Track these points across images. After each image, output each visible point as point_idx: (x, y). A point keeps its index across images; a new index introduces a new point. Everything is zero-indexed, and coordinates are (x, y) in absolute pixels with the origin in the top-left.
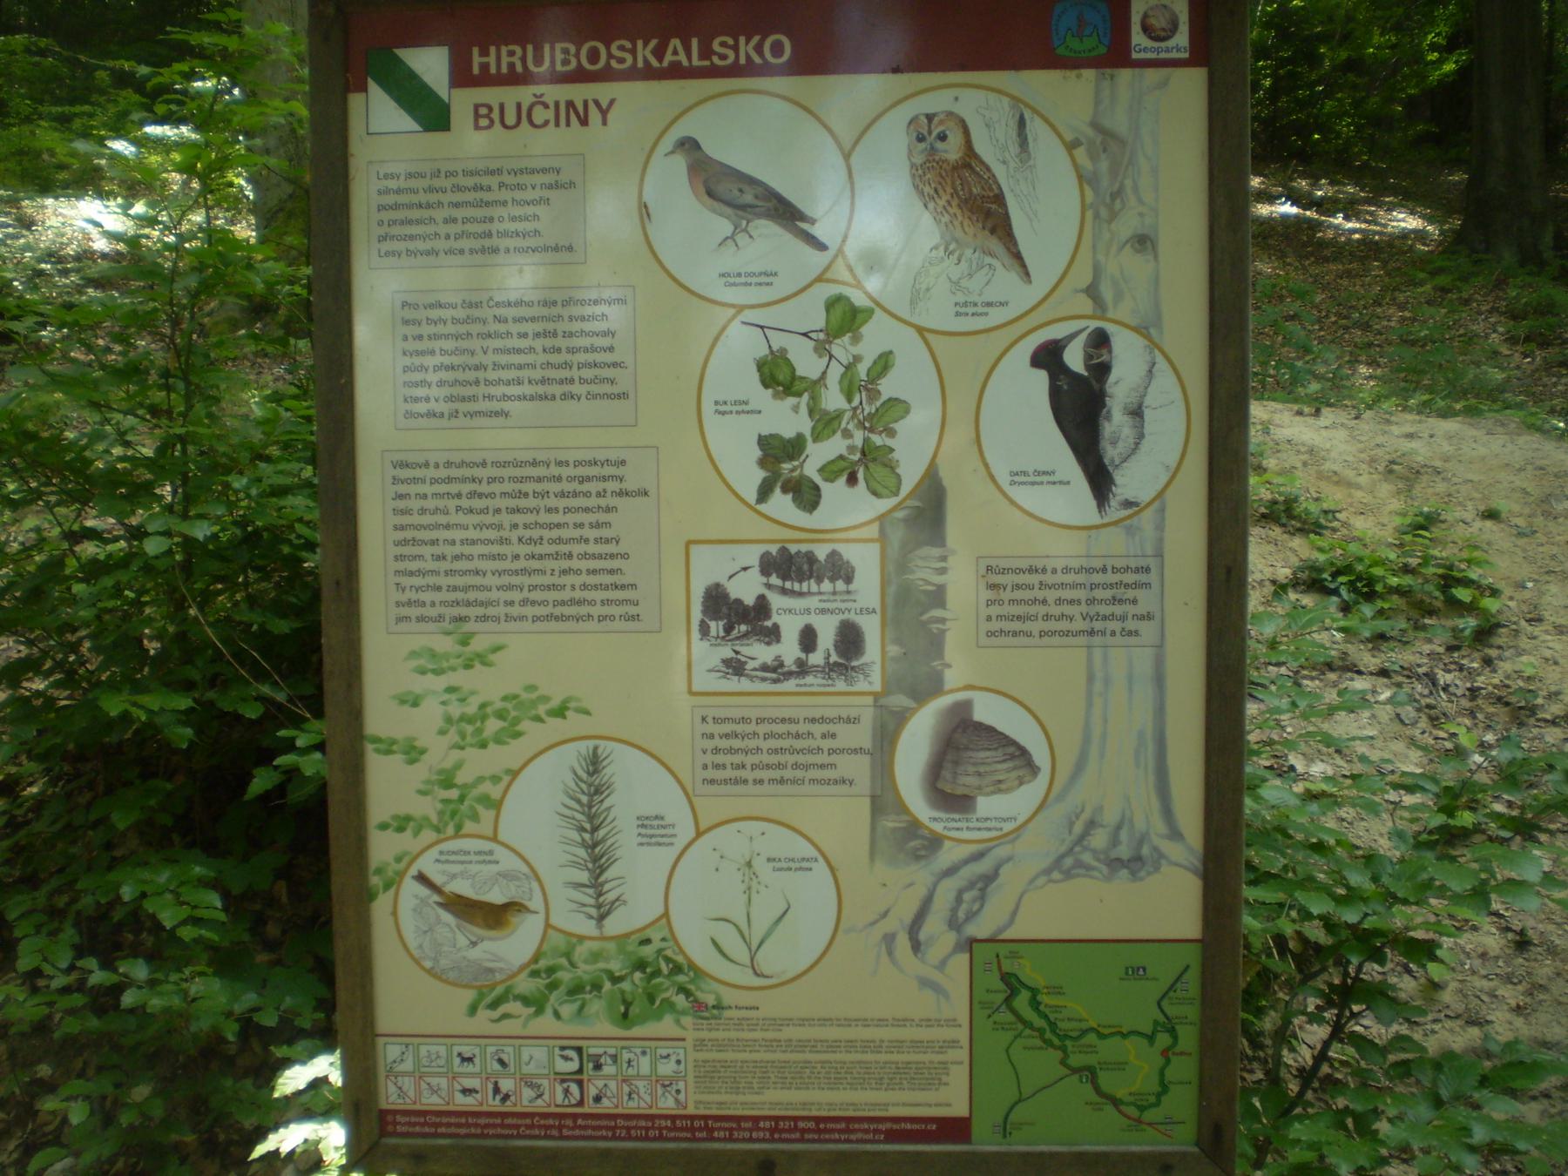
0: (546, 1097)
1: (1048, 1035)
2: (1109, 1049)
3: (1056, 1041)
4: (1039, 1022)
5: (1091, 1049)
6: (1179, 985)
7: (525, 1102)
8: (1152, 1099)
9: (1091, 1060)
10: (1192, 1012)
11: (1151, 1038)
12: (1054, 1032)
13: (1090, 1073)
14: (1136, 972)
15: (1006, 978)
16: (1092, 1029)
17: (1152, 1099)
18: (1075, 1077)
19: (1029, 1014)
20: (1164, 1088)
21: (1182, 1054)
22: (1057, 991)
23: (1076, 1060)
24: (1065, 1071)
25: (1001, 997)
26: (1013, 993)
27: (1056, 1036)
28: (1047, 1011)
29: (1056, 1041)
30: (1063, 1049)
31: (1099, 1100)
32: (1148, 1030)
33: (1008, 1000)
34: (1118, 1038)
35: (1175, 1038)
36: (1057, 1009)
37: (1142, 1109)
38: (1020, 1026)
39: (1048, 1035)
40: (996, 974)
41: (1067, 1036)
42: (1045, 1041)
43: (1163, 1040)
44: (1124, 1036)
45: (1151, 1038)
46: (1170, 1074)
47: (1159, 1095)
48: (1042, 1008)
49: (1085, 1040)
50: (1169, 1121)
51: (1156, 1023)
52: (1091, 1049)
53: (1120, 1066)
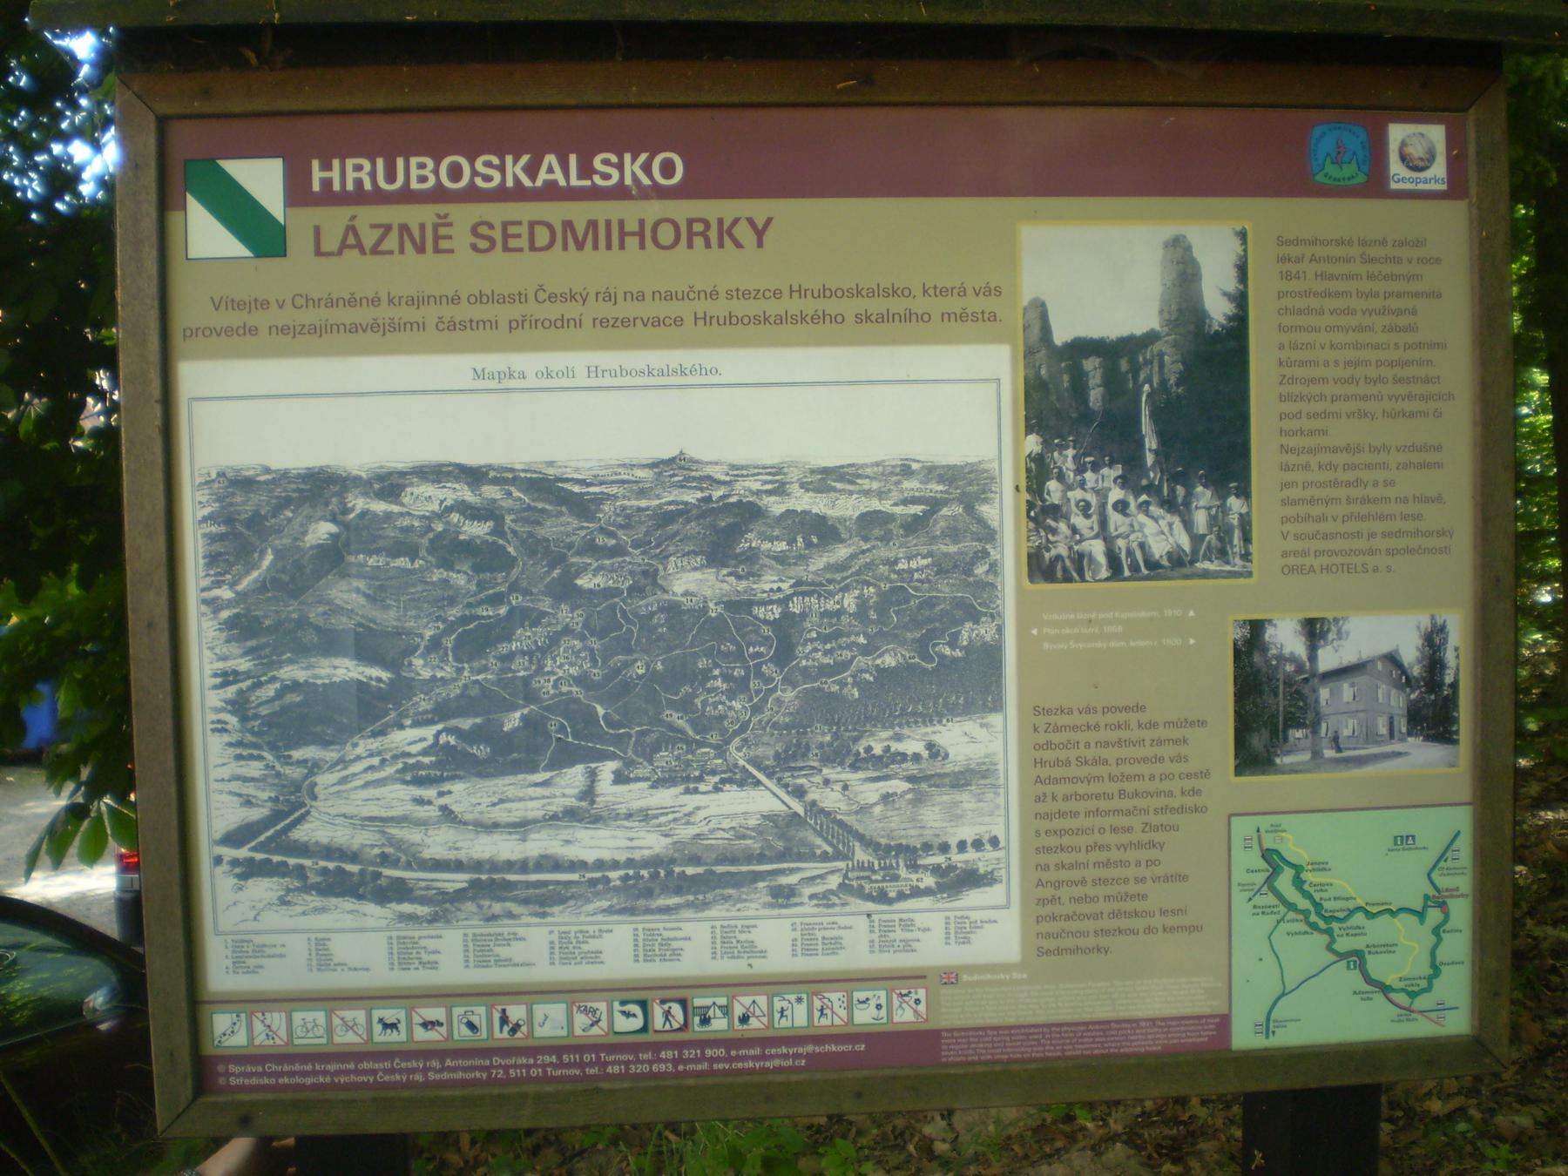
0: (604, 1023)
1: (1313, 918)
2: (1378, 930)
3: (1322, 925)
4: (1304, 904)
6: (1449, 854)
7: (578, 1032)
8: (1424, 984)
10: (1463, 882)
11: (1421, 915)
12: (1318, 914)
15: (1267, 855)
16: (1360, 908)
17: (1424, 984)
18: (1344, 962)
20: (1436, 969)
22: (1321, 867)
23: (1343, 945)
24: (1333, 958)
25: (1260, 878)
26: (1275, 872)
28: (1311, 890)
29: (1322, 925)
30: (1329, 932)
32: (1418, 906)
33: (1270, 880)
34: (1387, 916)
36: (1322, 887)
37: (1413, 995)
38: (1283, 909)
39: (1313, 918)
40: (1256, 852)
41: (1334, 918)
43: (1434, 915)
44: (1393, 913)
46: (1441, 955)
48: (1306, 887)
50: (1441, 1007)
51: (1426, 897)
52: (1359, 931)
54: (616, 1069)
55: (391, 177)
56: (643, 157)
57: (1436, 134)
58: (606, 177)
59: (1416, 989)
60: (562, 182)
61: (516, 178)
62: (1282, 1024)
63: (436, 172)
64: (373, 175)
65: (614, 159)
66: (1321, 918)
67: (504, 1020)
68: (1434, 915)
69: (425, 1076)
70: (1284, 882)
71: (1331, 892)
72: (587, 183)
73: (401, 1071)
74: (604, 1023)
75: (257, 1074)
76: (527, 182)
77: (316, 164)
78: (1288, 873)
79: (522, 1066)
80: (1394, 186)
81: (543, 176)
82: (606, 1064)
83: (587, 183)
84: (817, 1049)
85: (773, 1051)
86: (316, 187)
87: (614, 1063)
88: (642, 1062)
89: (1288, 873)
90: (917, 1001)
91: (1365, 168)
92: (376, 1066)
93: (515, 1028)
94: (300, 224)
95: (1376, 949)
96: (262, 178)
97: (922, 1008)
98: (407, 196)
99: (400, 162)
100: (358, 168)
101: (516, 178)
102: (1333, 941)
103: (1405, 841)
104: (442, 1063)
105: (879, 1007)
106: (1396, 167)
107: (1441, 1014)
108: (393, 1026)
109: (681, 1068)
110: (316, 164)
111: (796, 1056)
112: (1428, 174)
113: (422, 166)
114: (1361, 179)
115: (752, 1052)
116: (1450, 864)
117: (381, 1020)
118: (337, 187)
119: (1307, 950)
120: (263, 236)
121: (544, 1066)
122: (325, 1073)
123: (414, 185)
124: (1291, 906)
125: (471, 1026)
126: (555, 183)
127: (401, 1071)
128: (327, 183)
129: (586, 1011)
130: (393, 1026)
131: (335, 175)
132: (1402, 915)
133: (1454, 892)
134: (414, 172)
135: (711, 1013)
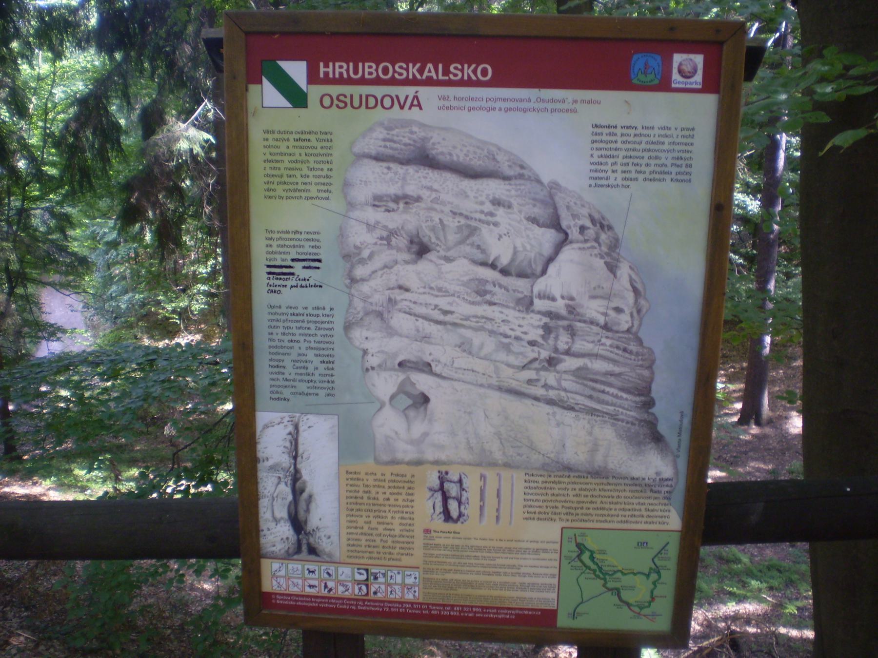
1: (598, 573)
2: (627, 580)
3: (601, 576)
4: (594, 567)
8: (646, 604)
9: (618, 585)
11: (648, 576)
12: (601, 571)
13: (617, 591)
14: (643, 544)
15: (578, 545)
16: (618, 571)
19: (588, 562)
20: (653, 599)
21: (662, 583)
23: (610, 585)
25: (575, 555)
26: (582, 552)
27: (601, 573)
29: (601, 576)
31: (619, 603)
33: (579, 556)
34: (631, 575)
35: (660, 577)
36: (603, 560)
37: (641, 608)
38: (584, 568)
40: (574, 544)
43: (654, 576)
44: (635, 574)
45: (648, 576)
46: (655, 593)
50: (654, 614)
51: (651, 569)
53: (632, 588)
68: (654, 576)
70: (586, 557)
71: (607, 563)
95: (626, 588)
97: (417, 594)
102: (606, 582)
119: (597, 585)
133: (665, 568)
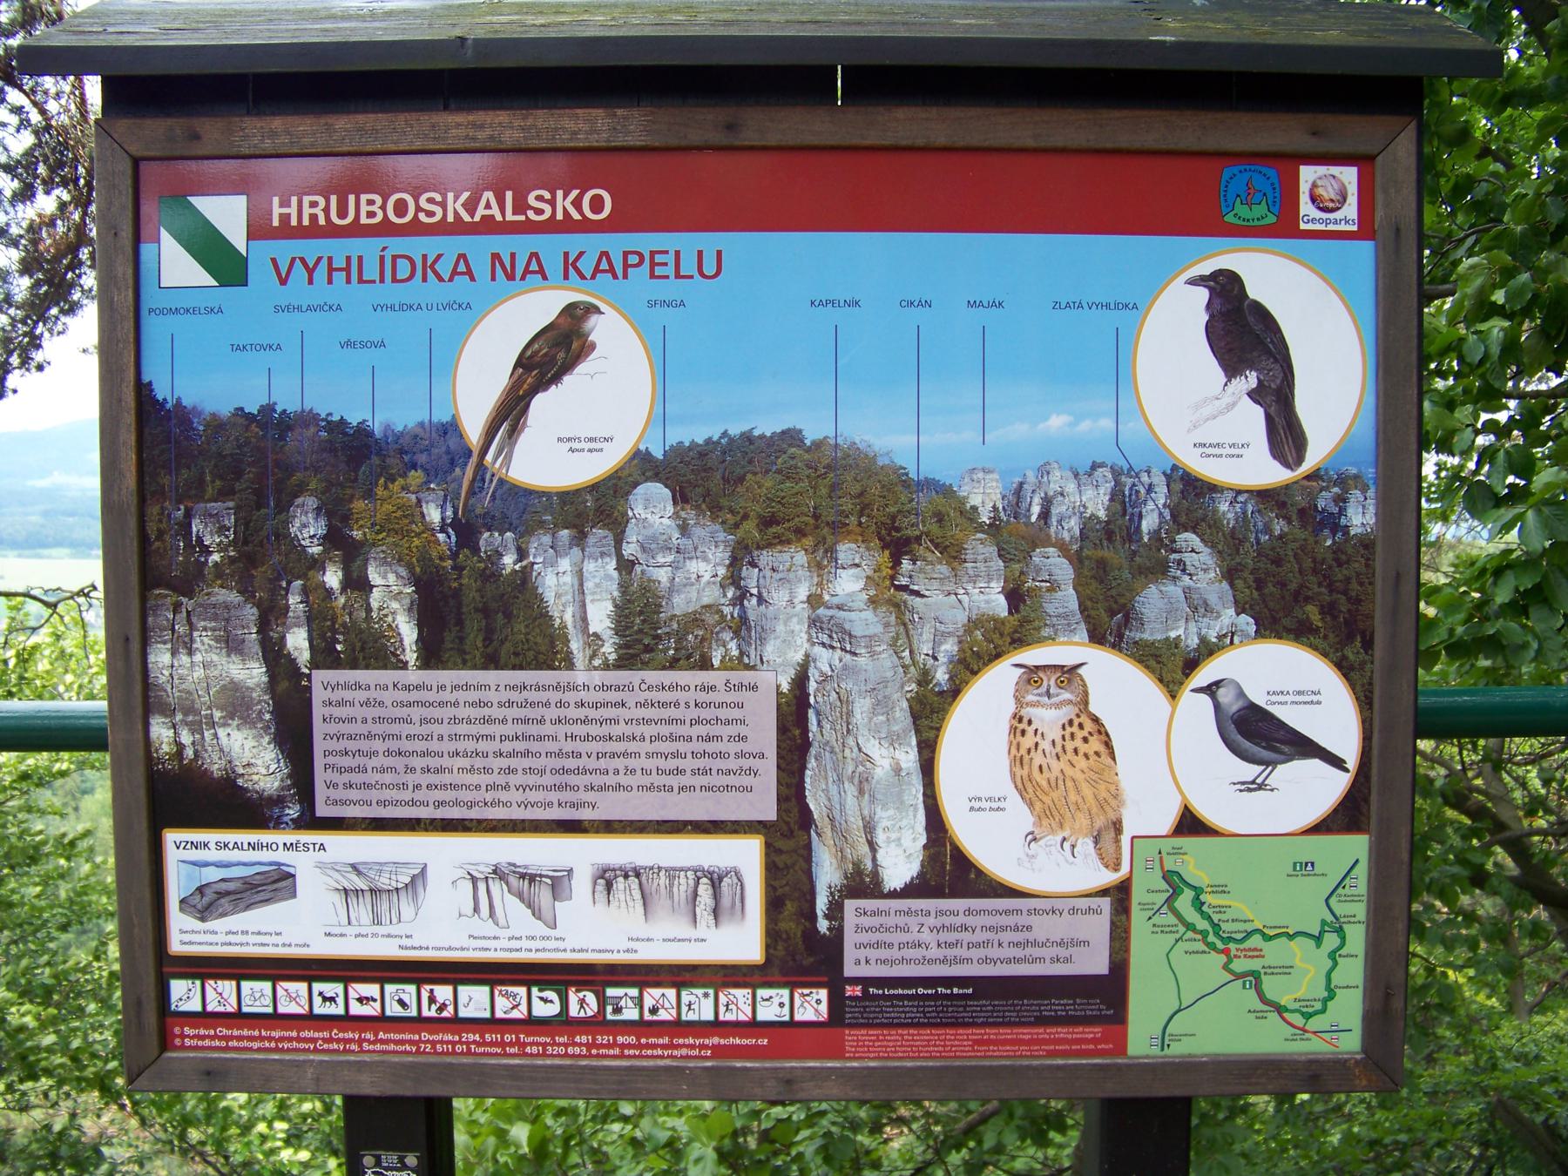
1: (1211, 938)
2: (1274, 952)
3: (1220, 945)
4: (1202, 924)
5: (1257, 953)
9: (1254, 965)
10: (1360, 910)
11: (1318, 939)
12: (1216, 934)
17: (1318, 1006)
19: (1191, 915)
20: (1331, 995)
22: (1221, 890)
23: (1239, 965)
26: (1175, 893)
28: (1210, 911)
29: (1220, 945)
30: (1226, 952)
33: (1169, 901)
35: (1343, 939)
36: (1221, 909)
37: (1308, 1016)
38: (1182, 929)
39: (1211, 938)
41: (1230, 939)
42: (1208, 944)
43: (1331, 940)
44: (1291, 937)
45: (1318, 939)
47: (1325, 1001)
48: (1205, 908)
49: (1248, 944)
51: (1324, 922)
52: (1257, 953)
53: (1286, 970)
54: (535, 1050)
55: (342, 214)
56: (575, 193)
57: (1349, 175)
58: (540, 212)
59: (1310, 1010)
60: (499, 218)
61: (456, 213)
62: (1177, 1038)
63: (384, 208)
64: (327, 210)
65: (547, 196)
66: (1220, 939)
67: (432, 1000)
68: (1331, 940)
69: (360, 1046)
70: (1184, 902)
72: (522, 218)
73: (338, 1041)
74: (523, 1008)
75: (209, 1037)
76: (467, 218)
77: (276, 200)
78: (1188, 894)
79: (448, 1042)
80: (1303, 226)
81: (481, 211)
82: (525, 1045)
83: (522, 218)
84: (722, 1042)
85: (681, 1041)
86: (276, 223)
87: (532, 1044)
88: (559, 1045)
89: (1188, 894)
90: (819, 1002)
91: (1276, 210)
92: (316, 1035)
93: (443, 1007)
94: (260, 256)
95: (1272, 970)
96: (227, 214)
98: (356, 230)
99: (352, 198)
100: (314, 204)
101: (456, 213)
103: (1306, 867)
104: (376, 1035)
105: (781, 1005)
106: (1306, 207)
107: (1335, 1035)
108: (332, 999)
109: (594, 1052)
110: (276, 200)
111: (702, 1047)
112: (1338, 215)
113: (371, 202)
114: (1271, 219)
115: (661, 1041)
116: (1347, 891)
117: (321, 994)
118: (294, 222)
120: (225, 265)
121: (468, 1043)
122: (270, 1039)
123: (364, 220)
124: (1189, 926)
125: (402, 1003)
126: (493, 216)
127: (338, 1041)
128: (285, 219)
129: (507, 995)
130: (332, 999)
131: (293, 211)
132: (1299, 939)
134: (364, 209)
135: (622, 1003)
